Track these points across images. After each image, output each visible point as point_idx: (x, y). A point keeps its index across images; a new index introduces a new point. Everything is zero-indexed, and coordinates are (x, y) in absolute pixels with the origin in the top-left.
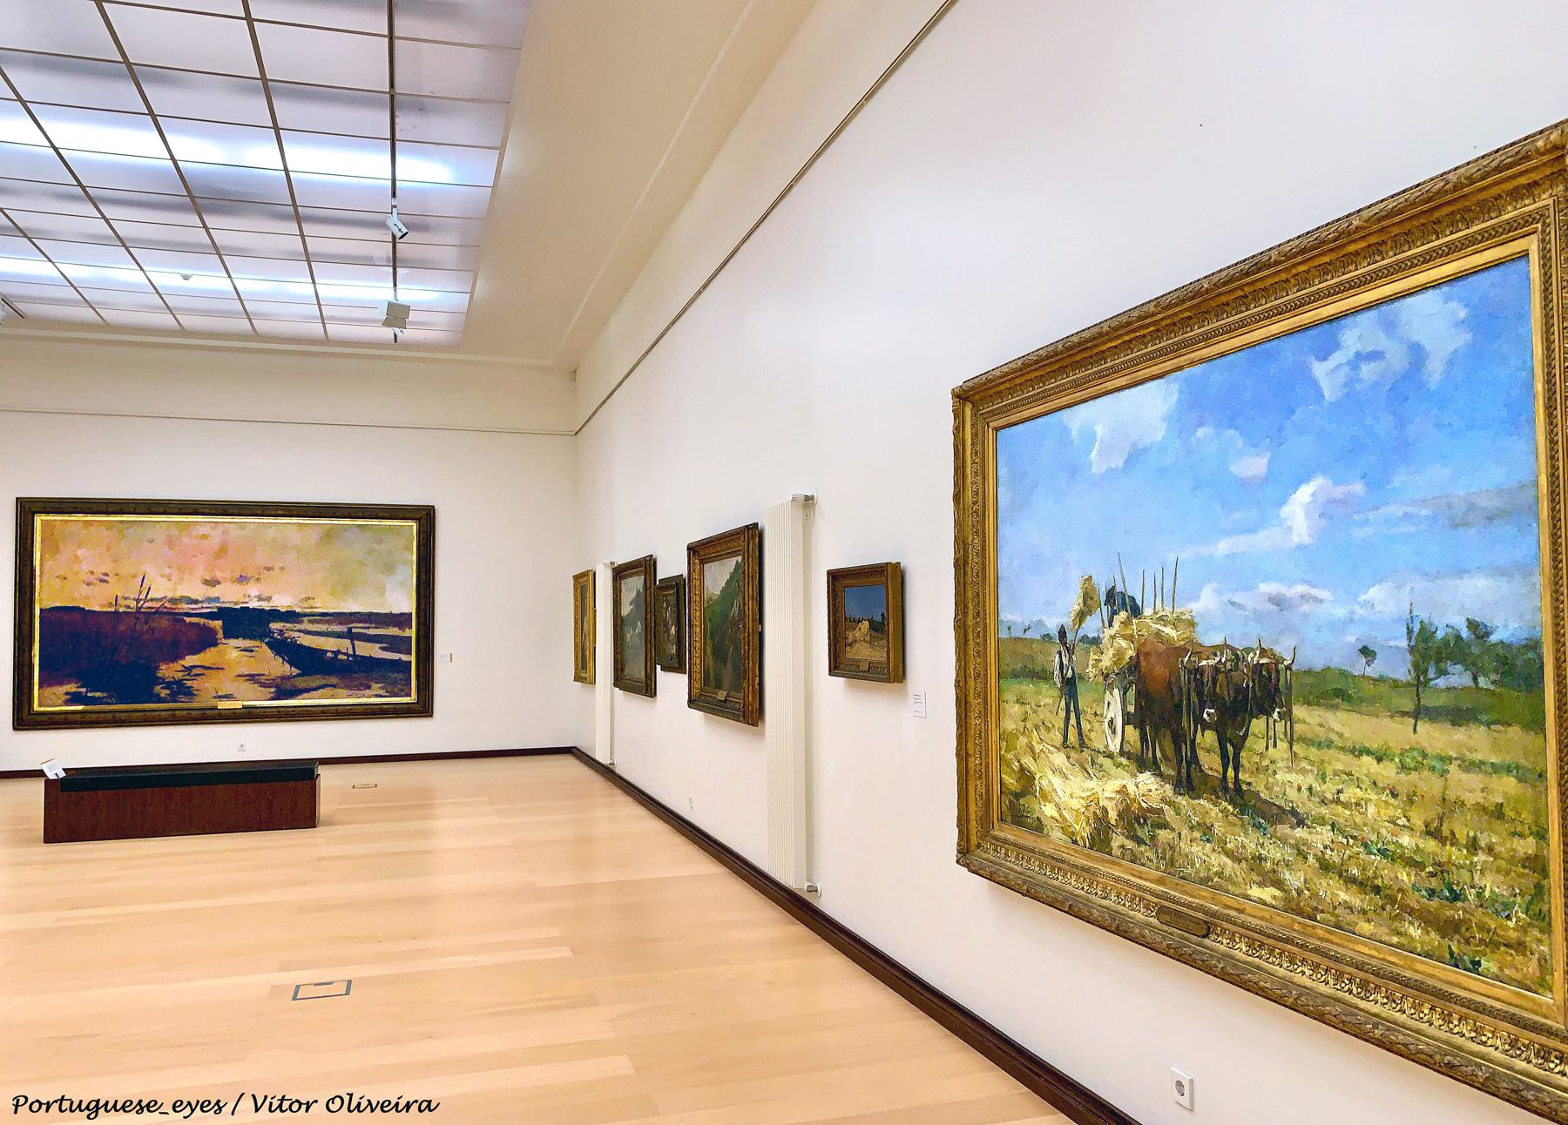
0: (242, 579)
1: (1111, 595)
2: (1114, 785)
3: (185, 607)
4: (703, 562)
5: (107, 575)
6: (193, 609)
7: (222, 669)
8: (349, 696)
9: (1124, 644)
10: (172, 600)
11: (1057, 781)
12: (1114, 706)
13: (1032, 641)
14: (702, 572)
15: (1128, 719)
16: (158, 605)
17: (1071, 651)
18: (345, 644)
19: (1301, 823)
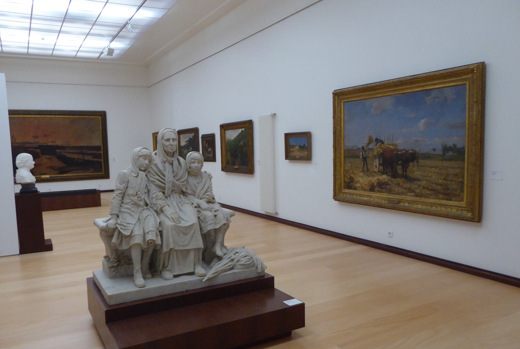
0: (45, 136)
1: (376, 140)
2: (376, 178)
4: (225, 130)
7: (42, 165)
8: (83, 173)
9: (379, 149)
11: (360, 179)
12: (377, 162)
13: (354, 150)
14: (225, 133)
15: (380, 165)
17: (365, 152)
18: (80, 156)
19: (419, 180)
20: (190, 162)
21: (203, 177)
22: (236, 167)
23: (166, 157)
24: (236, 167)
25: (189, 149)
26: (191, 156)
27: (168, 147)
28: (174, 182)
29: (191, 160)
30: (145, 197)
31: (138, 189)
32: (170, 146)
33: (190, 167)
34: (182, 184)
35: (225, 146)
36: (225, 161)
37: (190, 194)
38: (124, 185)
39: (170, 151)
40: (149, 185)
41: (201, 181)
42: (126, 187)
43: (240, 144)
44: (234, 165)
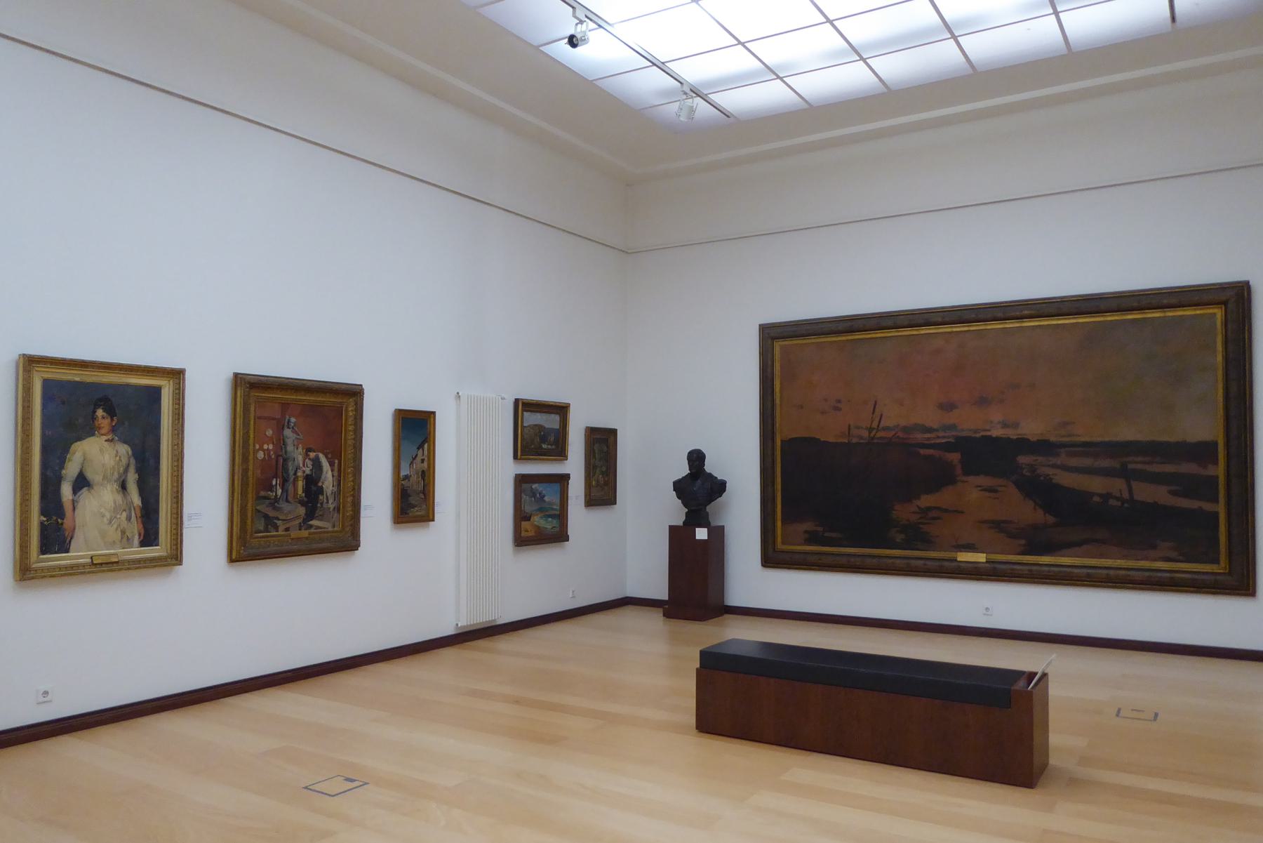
0: (983, 402)
3: (920, 437)
5: (839, 401)
6: (929, 439)
7: (962, 512)
8: (1125, 557)
10: (906, 429)
16: (890, 434)
18: (1117, 486)
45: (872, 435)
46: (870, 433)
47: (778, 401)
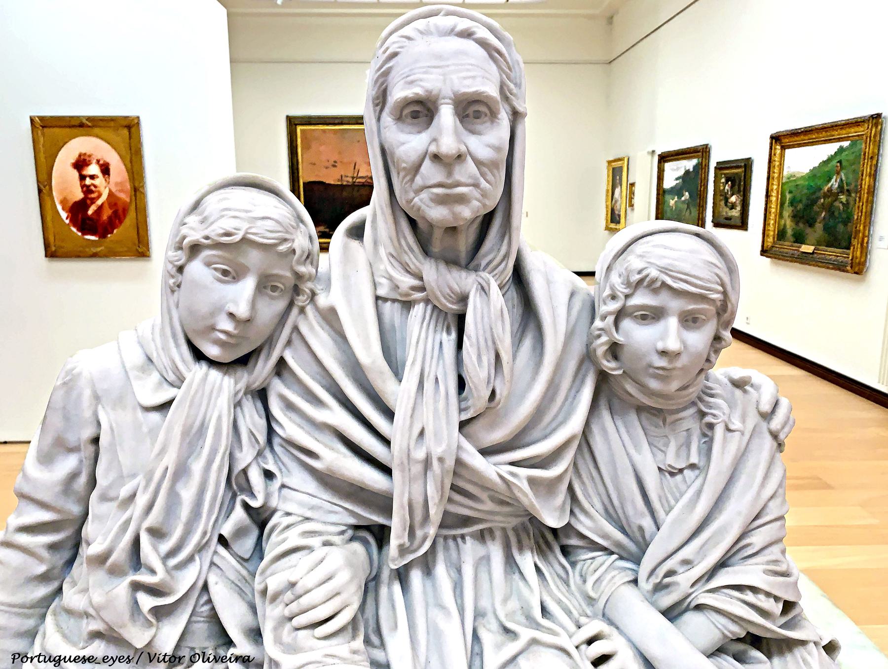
4: (783, 148)
14: (782, 156)
16: (363, 180)
20: (614, 306)
21: (719, 431)
22: (807, 248)
23: (415, 259)
24: (807, 248)
25: (683, 196)
26: (633, 262)
27: (419, 180)
28: (459, 462)
29: (627, 297)
30: (212, 579)
31: (147, 524)
32: (430, 172)
33: (614, 350)
34: (532, 481)
35: (778, 192)
36: (774, 231)
37: (595, 546)
38: (68, 464)
39: (437, 214)
40: (269, 475)
41: (694, 459)
42: (83, 479)
43: (830, 185)
44: (803, 243)
45: (354, 180)
46: (353, 179)
47: (300, 160)
